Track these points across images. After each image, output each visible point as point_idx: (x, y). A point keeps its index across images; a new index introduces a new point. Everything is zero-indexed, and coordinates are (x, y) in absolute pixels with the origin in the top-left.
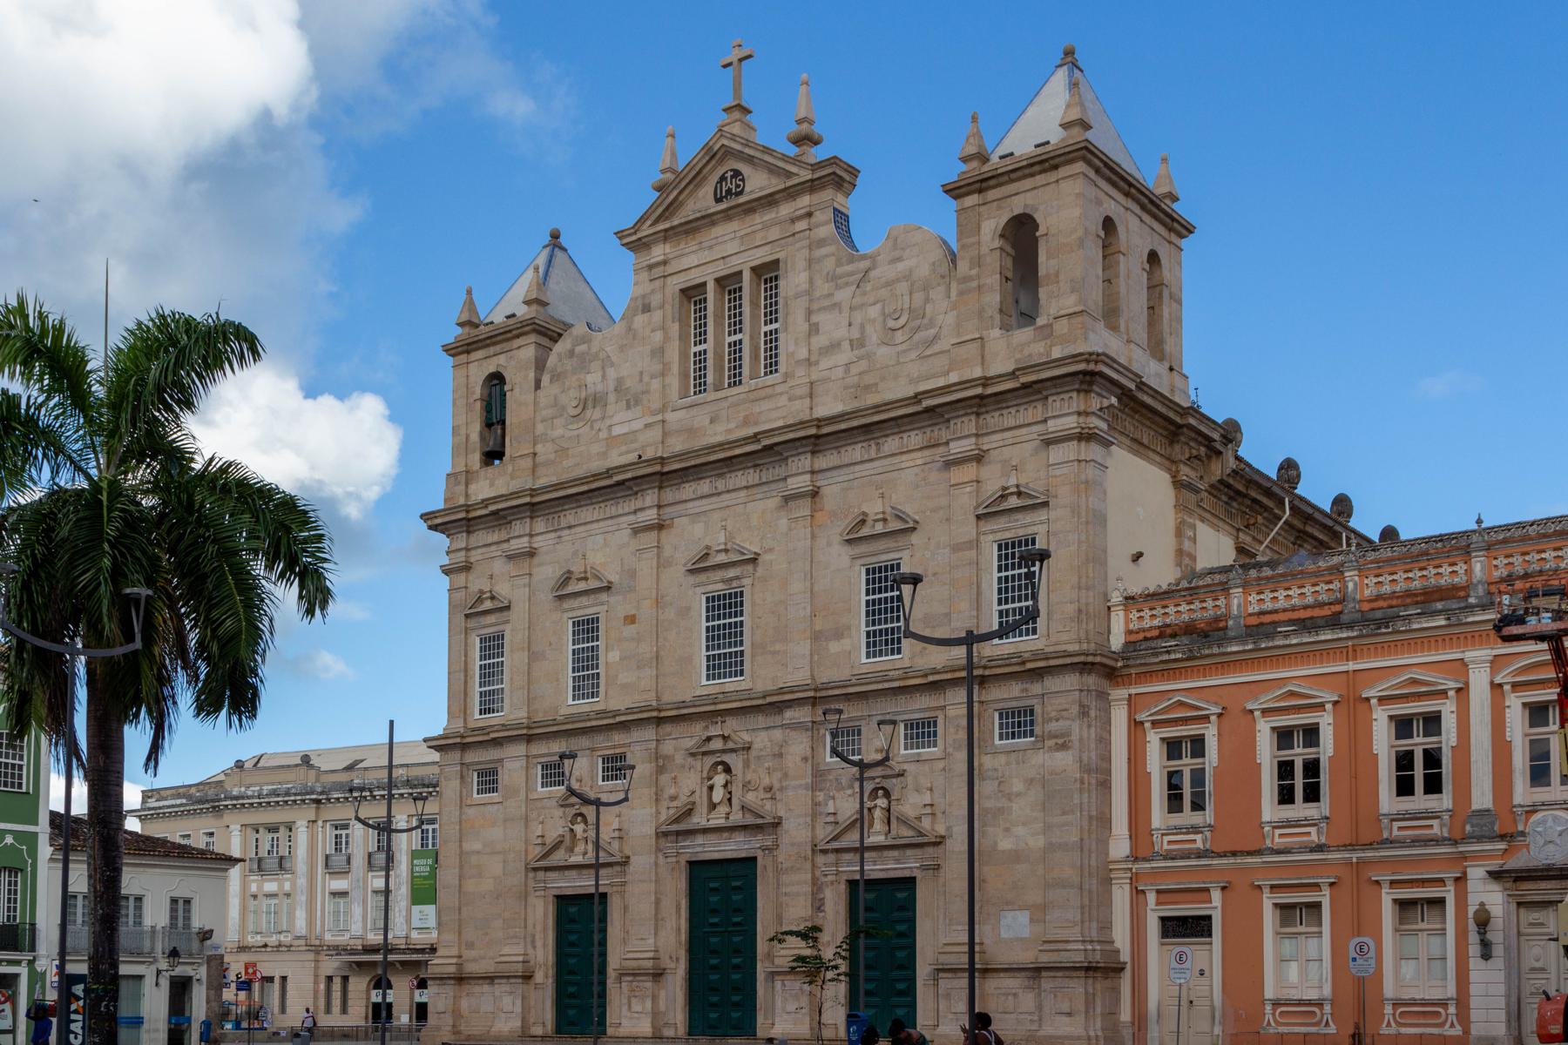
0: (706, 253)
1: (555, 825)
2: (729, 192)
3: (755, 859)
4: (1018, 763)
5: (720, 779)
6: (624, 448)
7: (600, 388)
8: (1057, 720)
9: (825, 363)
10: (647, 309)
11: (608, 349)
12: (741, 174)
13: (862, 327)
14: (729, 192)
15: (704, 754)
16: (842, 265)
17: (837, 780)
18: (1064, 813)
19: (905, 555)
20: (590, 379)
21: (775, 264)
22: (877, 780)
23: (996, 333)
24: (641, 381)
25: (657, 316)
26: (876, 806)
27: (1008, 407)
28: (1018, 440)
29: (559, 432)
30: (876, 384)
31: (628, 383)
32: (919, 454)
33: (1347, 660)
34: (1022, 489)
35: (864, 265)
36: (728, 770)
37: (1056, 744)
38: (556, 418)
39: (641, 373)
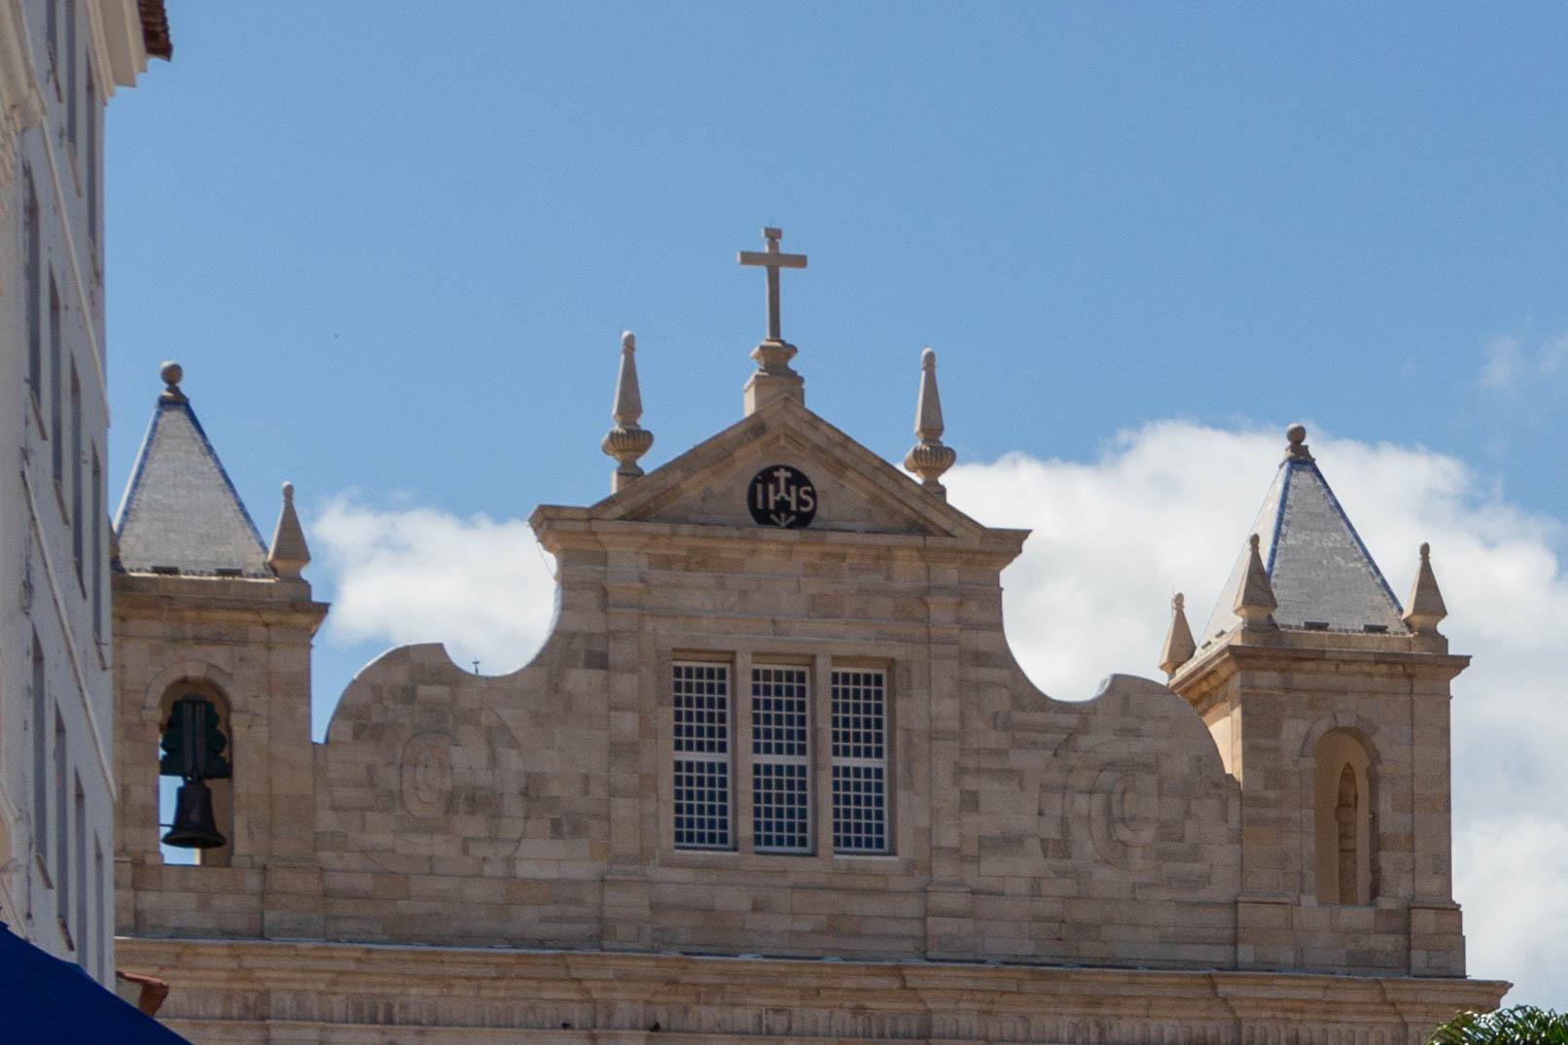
2: (783, 505)
6: (551, 910)
7: (484, 779)
9: (992, 868)
10: (599, 661)
11: (506, 714)
12: (810, 484)
13: (1064, 823)
14: (783, 505)
16: (1023, 709)
20: (457, 755)
23: (1309, 901)
24: (586, 792)
25: (625, 685)
29: (381, 840)
30: (1098, 927)
31: (555, 789)
35: (1072, 720)
38: (372, 809)
39: (587, 778)
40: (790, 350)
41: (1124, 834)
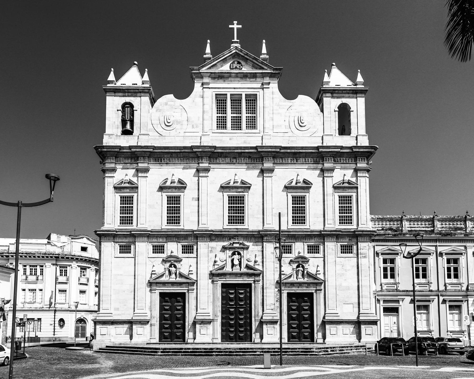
3: (251, 284)
4: (348, 261)
5: (236, 257)
8: (363, 249)
17: (284, 260)
18: (365, 276)
19: (307, 194)
22: (300, 262)
26: (299, 270)
27: (343, 157)
28: (345, 167)
32: (312, 165)
33: (437, 242)
34: (349, 181)
36: (239, 254)
37: (363, 256)
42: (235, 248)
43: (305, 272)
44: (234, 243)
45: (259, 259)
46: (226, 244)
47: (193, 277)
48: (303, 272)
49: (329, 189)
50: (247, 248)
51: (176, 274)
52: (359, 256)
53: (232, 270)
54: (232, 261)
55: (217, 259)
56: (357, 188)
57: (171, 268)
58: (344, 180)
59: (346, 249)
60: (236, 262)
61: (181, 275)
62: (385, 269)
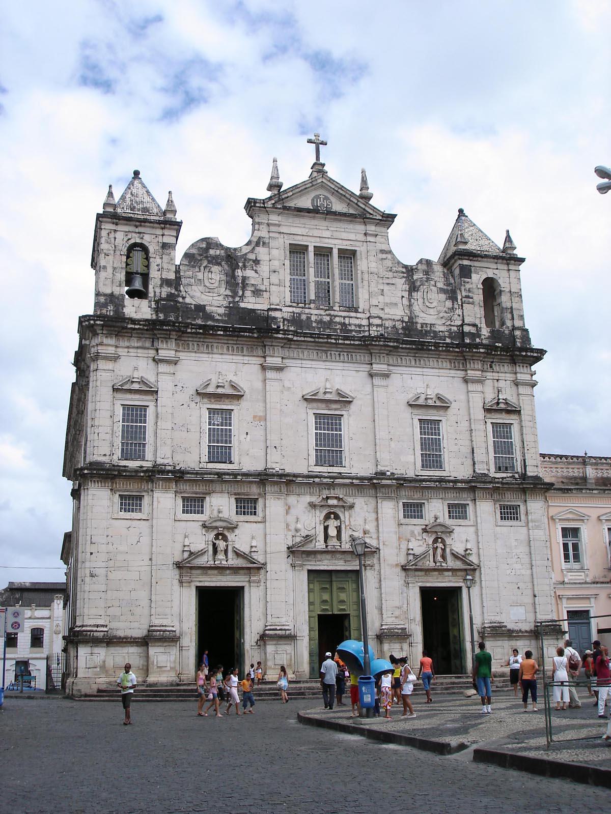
0: (307, 230)
1: (200, 541)
5: (333, 524)
15: (322, 506)
21: (354, 253)
32: (448, 371)
36: (337, 517)
40: (323, 165)
41: (428, 304)
42: (329, 506)
43: (448, 550)
44: (328, 498)
45: (370, 527)
46: (315, 499)
47: (259, 557)
48: (444, 550)
49: (479, 414)
50: (352, 507)
51: (226, 552)
52: (530, 524)
53: (327, 546)
54: (326, 528)
55: (299, 526)
56: (519, 412)
57: (217, 542)
58: (499, 399)
59: (509, 513)
60: (332, 532)
61: (238, 554)
62: (565, 546)
